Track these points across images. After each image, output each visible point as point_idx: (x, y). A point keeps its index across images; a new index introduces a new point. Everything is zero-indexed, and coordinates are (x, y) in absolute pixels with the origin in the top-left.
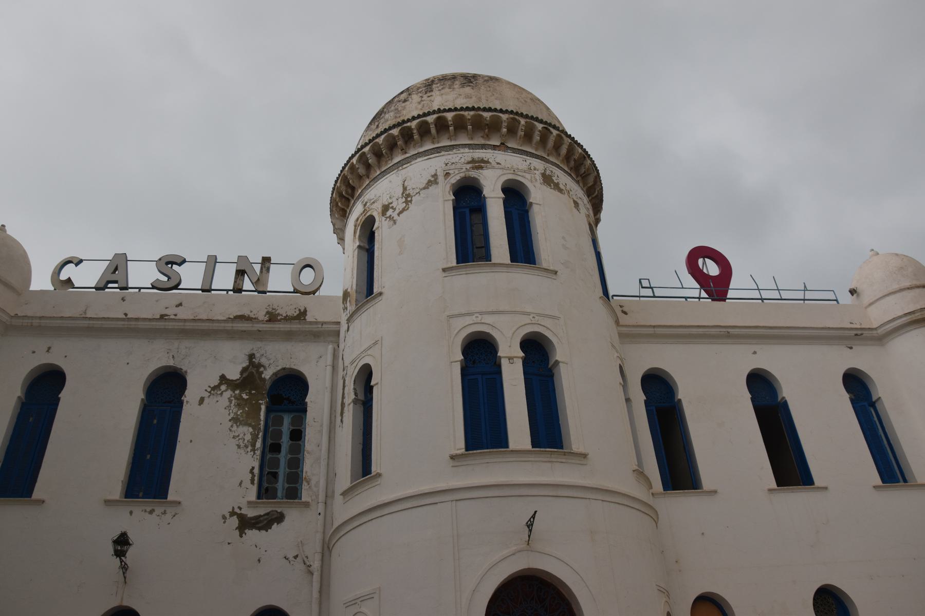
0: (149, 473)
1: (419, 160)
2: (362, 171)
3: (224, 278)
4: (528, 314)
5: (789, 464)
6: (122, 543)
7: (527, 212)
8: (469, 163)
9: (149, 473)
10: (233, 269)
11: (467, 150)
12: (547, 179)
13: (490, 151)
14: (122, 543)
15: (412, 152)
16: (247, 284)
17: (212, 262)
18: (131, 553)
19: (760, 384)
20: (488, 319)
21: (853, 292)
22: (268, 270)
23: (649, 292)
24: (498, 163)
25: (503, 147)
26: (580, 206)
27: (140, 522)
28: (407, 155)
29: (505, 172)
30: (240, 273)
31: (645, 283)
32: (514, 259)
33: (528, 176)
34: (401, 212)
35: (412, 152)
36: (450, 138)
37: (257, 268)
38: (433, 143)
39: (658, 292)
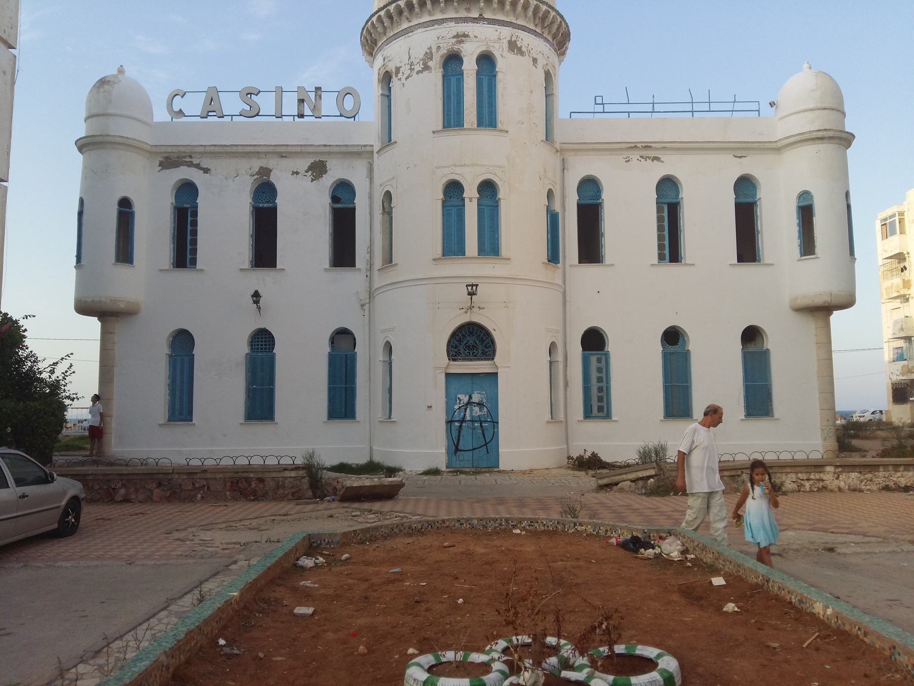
0: (264, 252)
1: (420, 30)
2: (380, 30)
3: (290, 106)
4: (483, 166)
5: (671, 248)
6: (256, 295)
7: (495, 76)
8: (454, 37)
9: (264, 252)
10: (294, 97)
11: (453, 24)
12: (513, 46)
13: (470, 24)
14: (256, 295)
15: (415, 22)
16: (307, 111)
17: (280, 92)
18: (262, 300)
19: (668, 188)
20: (458, 170)
21: (772, 104)
22: (320, 97)
23: (599, 108)
24: (476, 37)
26: (539, 62)
27: (263, 279)
28: (412, 24)
29: (480, 44)
30: (301, 101)
31: (599, 100)
32: (480, 124)
33: (497, 46)
34: (407, 78)
35: (415, 22)
36: (443, 11)
37: (312, 95)
38: (430, 15)
39: (608, 108)
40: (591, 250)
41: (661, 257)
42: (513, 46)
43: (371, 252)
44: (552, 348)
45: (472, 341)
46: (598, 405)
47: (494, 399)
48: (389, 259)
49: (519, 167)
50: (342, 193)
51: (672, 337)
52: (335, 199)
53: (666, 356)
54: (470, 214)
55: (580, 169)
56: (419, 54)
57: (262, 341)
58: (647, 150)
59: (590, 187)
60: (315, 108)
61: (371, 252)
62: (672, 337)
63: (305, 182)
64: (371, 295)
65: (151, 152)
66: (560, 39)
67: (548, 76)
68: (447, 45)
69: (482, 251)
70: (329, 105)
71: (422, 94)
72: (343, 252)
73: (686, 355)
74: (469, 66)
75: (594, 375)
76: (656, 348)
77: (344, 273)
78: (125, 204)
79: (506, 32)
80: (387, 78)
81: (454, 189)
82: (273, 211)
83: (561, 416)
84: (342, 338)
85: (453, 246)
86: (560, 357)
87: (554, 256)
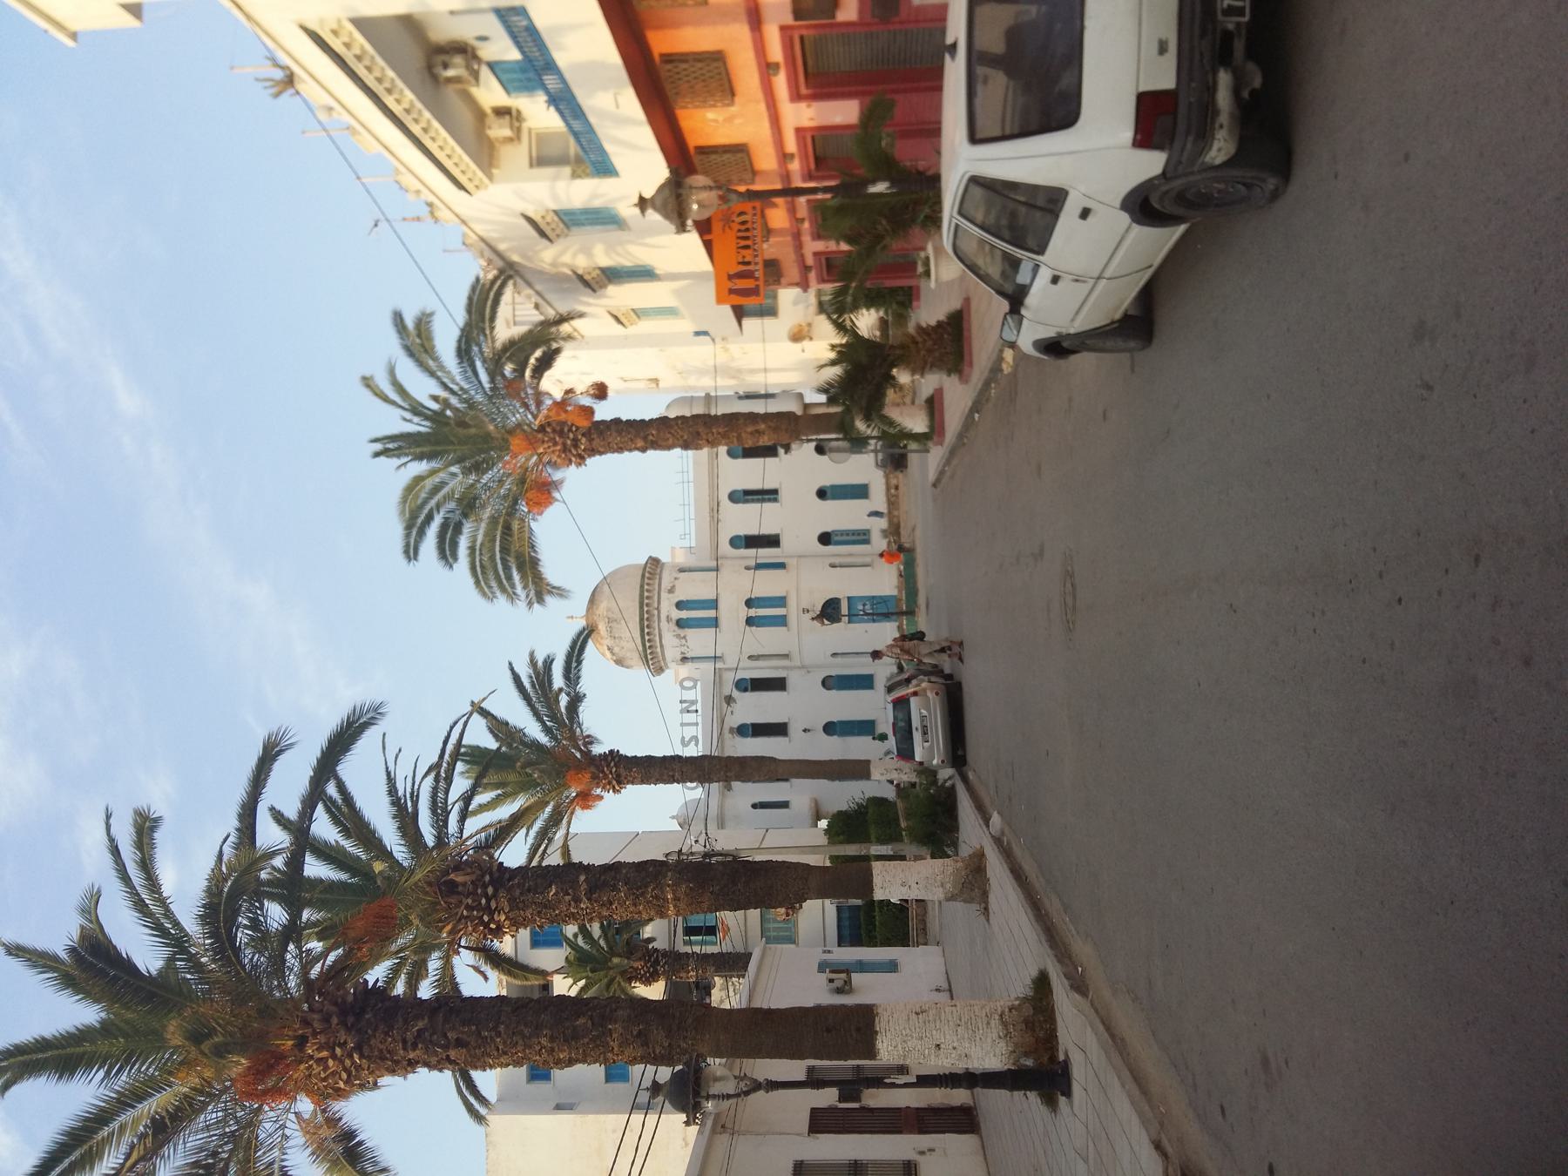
3: (691, 718)
5: (769, 495)
12: (671, 591)
17: (682, 725)
19: (735, 497)
25: (658, 609)
27: (795, 729)
40: (772, 541)
41: (775, 500)
42: (671, 591)
43: (776, 668)
44: (833, 566)
45: (830, 611)
46: (862, 537)
47: (861, 598)
48: (786, 656)
49: (736, 585)
50: (742, 686)
51: (822, 494)
52: (746, 690)
53: (834, 498)
54: (764, 612)
55: (725, 547)
56: (676, 641)
57: (830, 728)
58: (715, 509)
59: (735, 542)
60: (694, 702)
61: (776, 668)
62: (822, 494)
63: (737, 707)
64: (803, 667)
65: (723, 795)
66: (654, 562)
67: (682, 570)
68: (673, 626)
69: (784, 605)
70: (690, 695)
71: (700, 640)
72: (778, 684)
73: (833, 487)
74: (684, 614)
75: (845, 538)
76: (830, 504)
77: (789, 684)
78: (754, 806)
79: (664, 595)
80: (684, 659)
81: (750, 621)
82: (753, 725)
83: (867, 560)
84: (827, 683)
85: (781, 621)
86: (837, 561)
87: (782, 566)
